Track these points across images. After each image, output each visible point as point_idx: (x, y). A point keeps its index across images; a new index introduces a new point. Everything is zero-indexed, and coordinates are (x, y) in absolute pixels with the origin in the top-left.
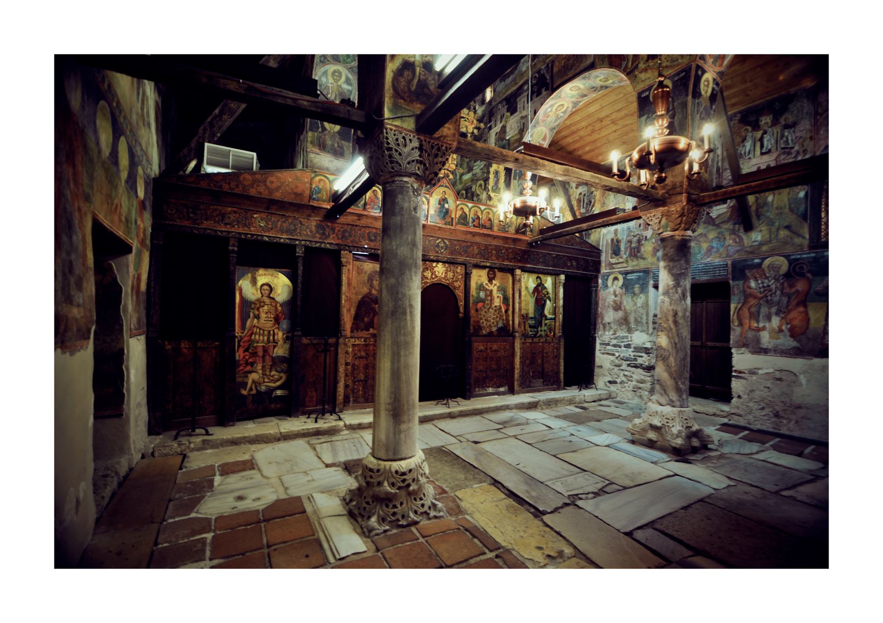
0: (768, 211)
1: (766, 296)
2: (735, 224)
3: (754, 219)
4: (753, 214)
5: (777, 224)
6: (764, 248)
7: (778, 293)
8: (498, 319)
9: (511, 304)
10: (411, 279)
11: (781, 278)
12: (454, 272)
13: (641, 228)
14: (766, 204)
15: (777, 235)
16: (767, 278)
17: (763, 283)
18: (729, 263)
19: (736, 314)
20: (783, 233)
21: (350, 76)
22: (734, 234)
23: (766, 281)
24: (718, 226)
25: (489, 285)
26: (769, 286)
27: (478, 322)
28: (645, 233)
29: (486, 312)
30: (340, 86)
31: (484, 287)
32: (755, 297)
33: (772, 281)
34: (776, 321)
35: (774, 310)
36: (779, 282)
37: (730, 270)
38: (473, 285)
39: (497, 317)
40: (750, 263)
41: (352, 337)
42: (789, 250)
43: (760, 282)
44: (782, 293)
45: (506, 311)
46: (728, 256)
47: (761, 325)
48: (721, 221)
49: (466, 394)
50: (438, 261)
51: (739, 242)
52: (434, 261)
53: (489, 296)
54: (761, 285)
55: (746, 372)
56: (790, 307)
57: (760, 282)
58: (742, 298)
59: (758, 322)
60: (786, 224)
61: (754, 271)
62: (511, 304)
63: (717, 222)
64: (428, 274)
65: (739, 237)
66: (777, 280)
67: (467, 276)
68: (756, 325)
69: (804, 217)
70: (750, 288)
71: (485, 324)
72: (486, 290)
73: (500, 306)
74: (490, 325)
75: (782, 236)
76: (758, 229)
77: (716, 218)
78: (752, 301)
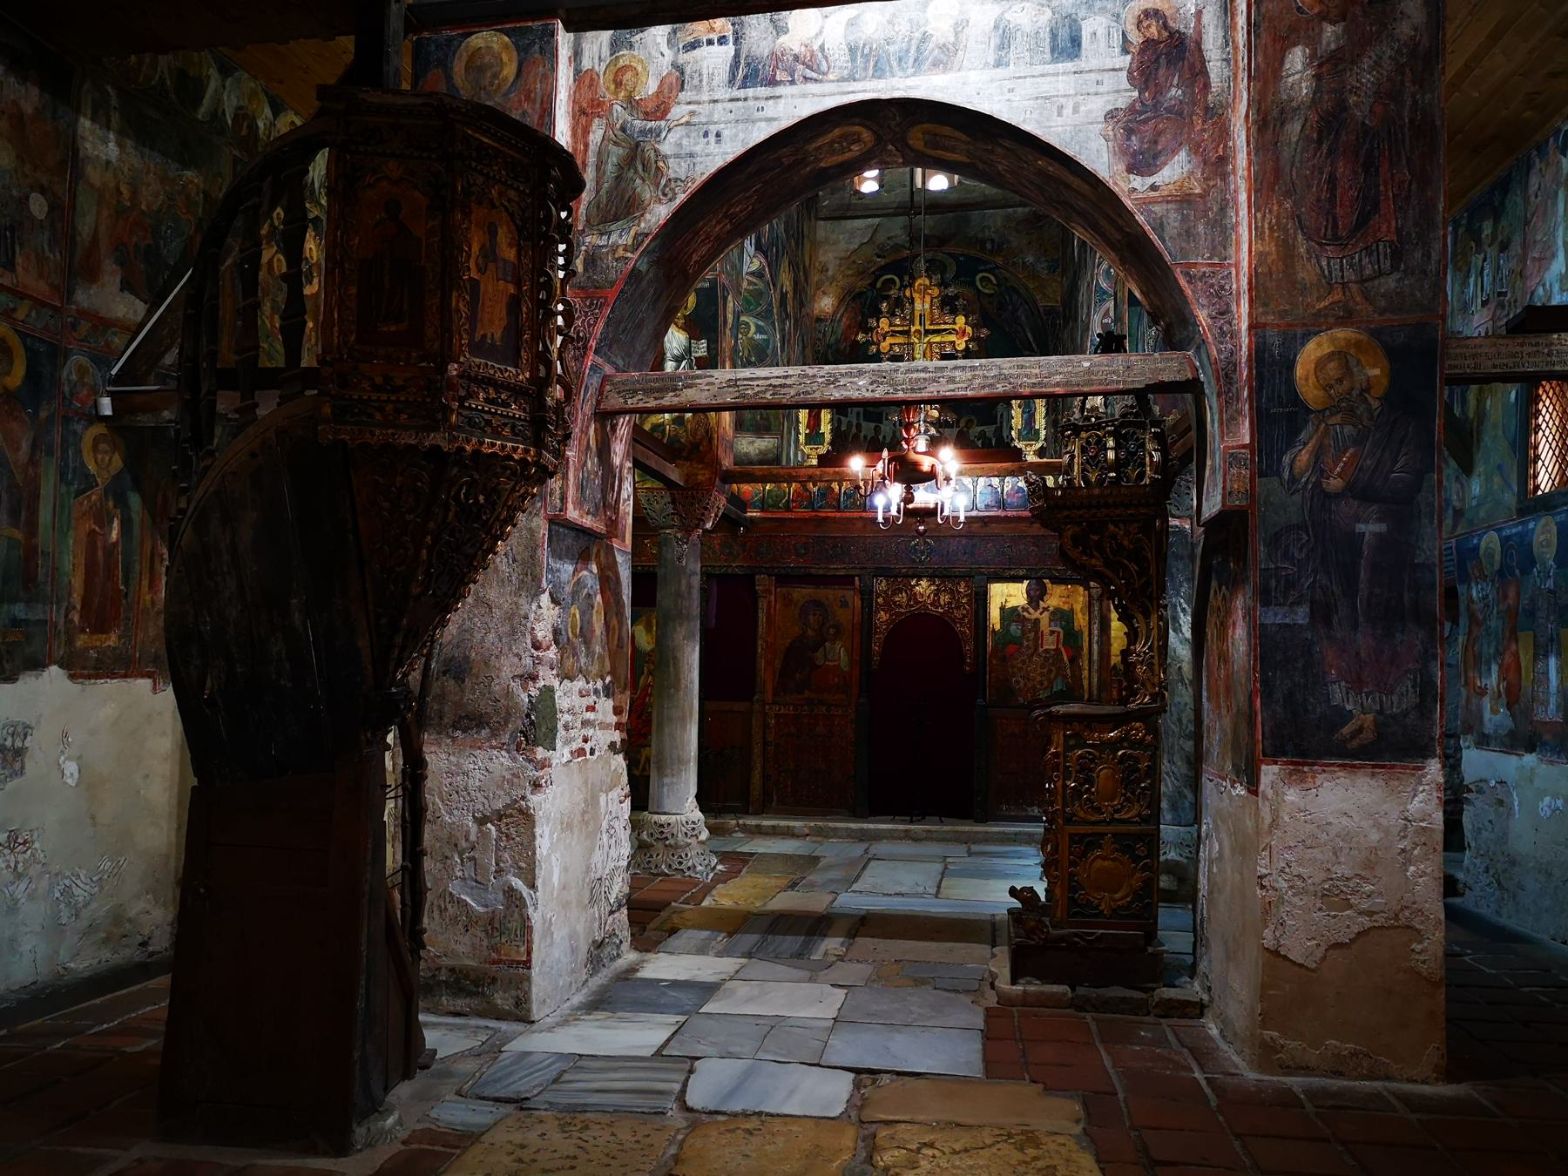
8: (1052, 676)
9: (1086, 645)
10: (675, 630)
12: (952, 592)
21: (760, 323)
25: (1031, 610)
29: (1024, 662)
30: (752, 338)
31: (1019, 615)
39: (1050, 671)
41: (774, 703)
45: (1074, 660)
49: (984, 819)
50: (920, 578)
52: (913, 577)
53: (1030, 631)
62: (1086, 645)
64: (902, 598)
67: (982, 599)
71: (1022, 684)
73: (1057, 649)
74: (1034, 687)
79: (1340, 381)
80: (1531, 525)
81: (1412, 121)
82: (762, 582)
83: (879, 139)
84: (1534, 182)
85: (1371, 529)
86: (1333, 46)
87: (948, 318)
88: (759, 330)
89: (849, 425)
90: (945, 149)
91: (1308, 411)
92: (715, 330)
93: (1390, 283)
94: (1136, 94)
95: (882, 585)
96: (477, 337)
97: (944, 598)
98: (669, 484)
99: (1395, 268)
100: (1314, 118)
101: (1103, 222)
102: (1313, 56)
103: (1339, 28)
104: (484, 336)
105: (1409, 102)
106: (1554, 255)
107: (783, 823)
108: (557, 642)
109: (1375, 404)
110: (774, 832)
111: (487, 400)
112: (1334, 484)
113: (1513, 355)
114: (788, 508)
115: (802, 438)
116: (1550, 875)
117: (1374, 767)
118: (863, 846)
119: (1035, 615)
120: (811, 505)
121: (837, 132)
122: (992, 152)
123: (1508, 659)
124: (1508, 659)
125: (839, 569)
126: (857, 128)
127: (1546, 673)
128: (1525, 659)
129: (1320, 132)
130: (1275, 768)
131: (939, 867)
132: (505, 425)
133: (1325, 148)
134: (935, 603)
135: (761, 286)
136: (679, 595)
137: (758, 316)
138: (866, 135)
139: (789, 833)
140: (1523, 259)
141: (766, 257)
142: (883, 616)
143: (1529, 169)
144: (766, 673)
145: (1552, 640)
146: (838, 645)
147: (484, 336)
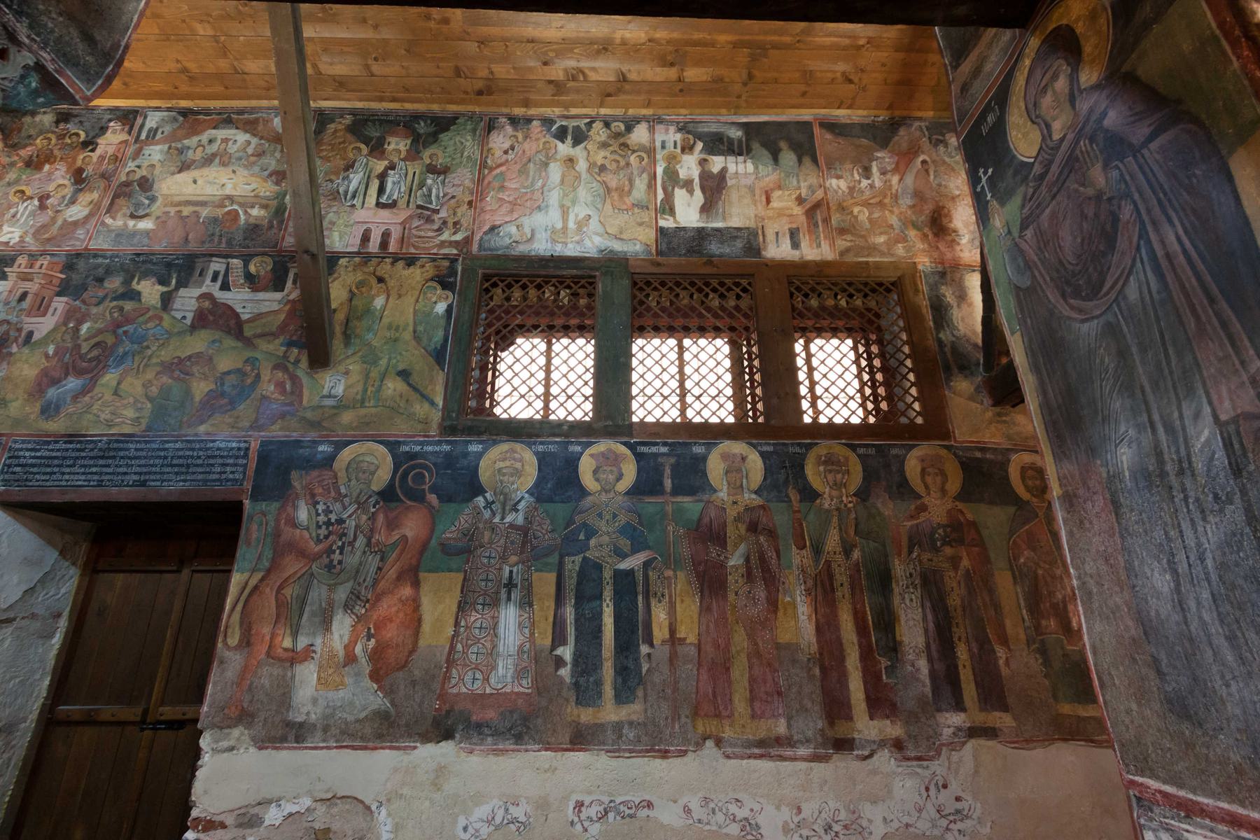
0: (369, 329)
1: (330, 551)
2: (290, 344)
3: (337, 344)
4: (338, 329)
5: (383, 362)
6: (347, 417)
7: (361, 542)
11: (372, 500)
13: (26, 304)
14: (368, 311)
15: (379, 389)
16: (340, 497)
17: (328, 511)
18: (255, 445)
19: (239, 608)
20: (394, 386)
22: (285, 369)
23: (338, 506)
24: (249, 343)
26: (340, 521)
28: (30, 323)
32: (302, 554)
33: (351, 510)
34: (342, 626)
35: (342, 594)
36: (365, 511)
37: (253, 465)
40: (305, 452)
42: (400, 428)
43: (320, 507)
44: (369, 544)
46: (255, 426)
47: (302, 642)
48: (259, 331)
51: (292, 393)
54: (322, 518)
55: (229, 820)
56: (382, 585)
57: (320, 507)
58: (268, 554)
59: (295, 635)
60: (401, 367)
61: (315, 473)
63: (248, 332)
65: (294, 379)
66: (361, 505)
68: (287, 643)
69: (438, 356)
70: (293, 523)
75: (390, 392)
76: (342, 368)
77: (248, 321)
78: (292, 566)
145: (510, 585)
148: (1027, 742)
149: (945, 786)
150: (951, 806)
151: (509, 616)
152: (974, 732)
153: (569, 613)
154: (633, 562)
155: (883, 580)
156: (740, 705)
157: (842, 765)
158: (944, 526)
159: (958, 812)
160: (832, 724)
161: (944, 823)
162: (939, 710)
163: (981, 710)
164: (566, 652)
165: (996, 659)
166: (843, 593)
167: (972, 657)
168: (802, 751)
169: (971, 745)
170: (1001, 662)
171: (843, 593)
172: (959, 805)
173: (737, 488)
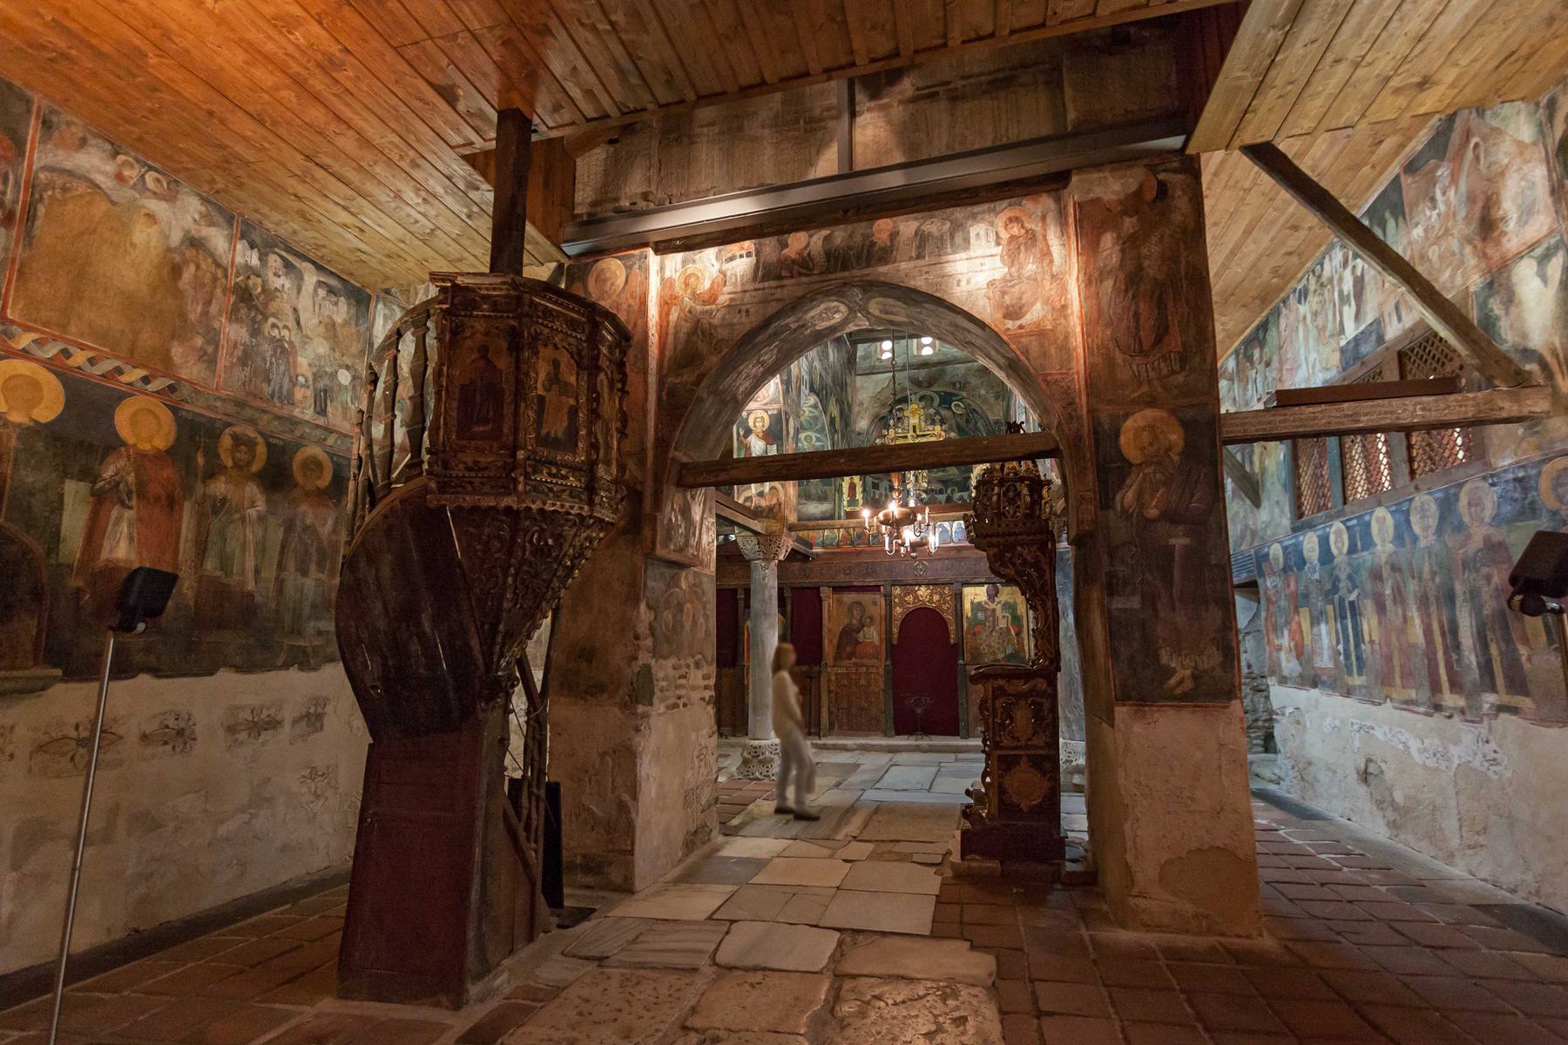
27: (977, 648)
38: (967, 606)
50: (920, 585)
64: (910, 598)
67: (959, 597)
72: (986, 610)
79: (1151, 444)
80: (1301, 538)
81: (1187, 274)
82: (825, 592)
83: (851, 310)
84: (1283, 322)
85: (1179, 541)
86: (1131, 231)
87: (931, 428)
88: (818, 440)
89: (881, 495)
90: (892, 313)
91: (1131, 465)
92: (781, 439)
93: (1180, 378)
94: (1006, 270)
95: (897, 591)
96: (544, 432)
97: (936, 598)
98: (756, 533)
99: (1182, 368)
100: (1122, 276)
101: (993, 353)
102: (1119, 237)
103: (1134, 220)
104: (548, 433)
105: (1184, 263)
106: (1299, 366)
107: (840, 742)
108: (653, 635)
109: (1176, 458)
110: (835, 748)
111: (550, 474)
112: (1153, 512)
113: (1270, 423)
114: (838, 546)
115: (845, 503)
116: (1335, 772)
117: (1194, 706)
118: (890, 755)
119: (992, 606)
120: (852, 543)
121: (823, 306)
122: (920, 313)
123: (1294, 626)
124: (1294, 626)
125: (870, 581)
126: (835, 303)
127: (1320, 635)
128: (1306, 626)
129: (1126, 285)
130: (1125, 709)
131: (934, 770)
132: (563, 491)
133: (1130, 295)
134: (931, 601)
135: (817, 413)
136: (764, 601)
137: (817, 431)
138: (843, 308)
139: (845, 749)
140: (1281, 370)
141: (818, 395)
142: (899, 610)
143: (1279, 314)
144: (829, 647)
146: (872, 629)
147: (548, 433)
148: (1543, 721)
149: (1487, 742)
150: (1492, 756)
151: (1323, 627)
152: (1501, 708)
153: (1339, 625)
154: (1353, 597)
155: (1450, 598)
156: (1398, 681)
157: (1438, 718)
158: (1481, 550)
159: (1494, 760)
160: (1433, 695)
161: (1486, 764)
162: (1483, 691)
163: (1508, 693)
164: (1341, 647)
165: (1520, 655)
166: (1433, 608)
167: (1501, 653)
168: (1422, 709)
169: (1504, 716)
170: (1523, 659)
171: (1433, 608)
172: (1495, 756)
173: (1383, 541)
